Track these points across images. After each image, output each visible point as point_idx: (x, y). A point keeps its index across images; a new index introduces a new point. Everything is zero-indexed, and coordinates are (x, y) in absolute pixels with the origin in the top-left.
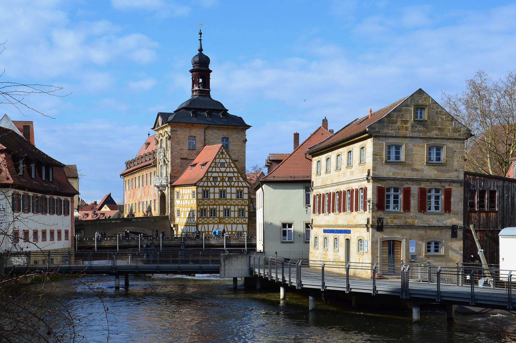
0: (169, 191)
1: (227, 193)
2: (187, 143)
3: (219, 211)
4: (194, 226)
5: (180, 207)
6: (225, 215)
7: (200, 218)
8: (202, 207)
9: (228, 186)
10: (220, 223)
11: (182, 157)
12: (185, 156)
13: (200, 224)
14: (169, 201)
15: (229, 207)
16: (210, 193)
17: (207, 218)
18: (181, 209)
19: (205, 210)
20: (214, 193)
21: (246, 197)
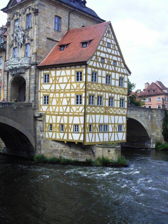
0: (33, 74)
1: (112, 79)
2: (54, 23)
3: (105, 99)
4: (79, 116)
5: (52, 92)
6: (110, 105)
7: (88, 106)
8: (90, 92)
9: (112, 71)
10: (105, 113)
11: (48, 36)
12: (51, 36)
13: (88, 113)
14: (32, 86)
15: (113, 95)
16: (98, 76)
17: (94, 106)
18: (51, 95)
19: (93, 97)
20: (102, 77)
21: (126, 85)
